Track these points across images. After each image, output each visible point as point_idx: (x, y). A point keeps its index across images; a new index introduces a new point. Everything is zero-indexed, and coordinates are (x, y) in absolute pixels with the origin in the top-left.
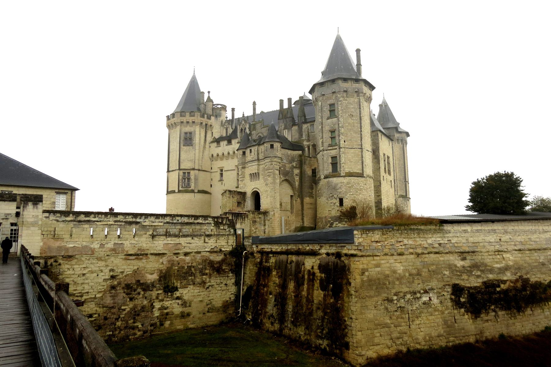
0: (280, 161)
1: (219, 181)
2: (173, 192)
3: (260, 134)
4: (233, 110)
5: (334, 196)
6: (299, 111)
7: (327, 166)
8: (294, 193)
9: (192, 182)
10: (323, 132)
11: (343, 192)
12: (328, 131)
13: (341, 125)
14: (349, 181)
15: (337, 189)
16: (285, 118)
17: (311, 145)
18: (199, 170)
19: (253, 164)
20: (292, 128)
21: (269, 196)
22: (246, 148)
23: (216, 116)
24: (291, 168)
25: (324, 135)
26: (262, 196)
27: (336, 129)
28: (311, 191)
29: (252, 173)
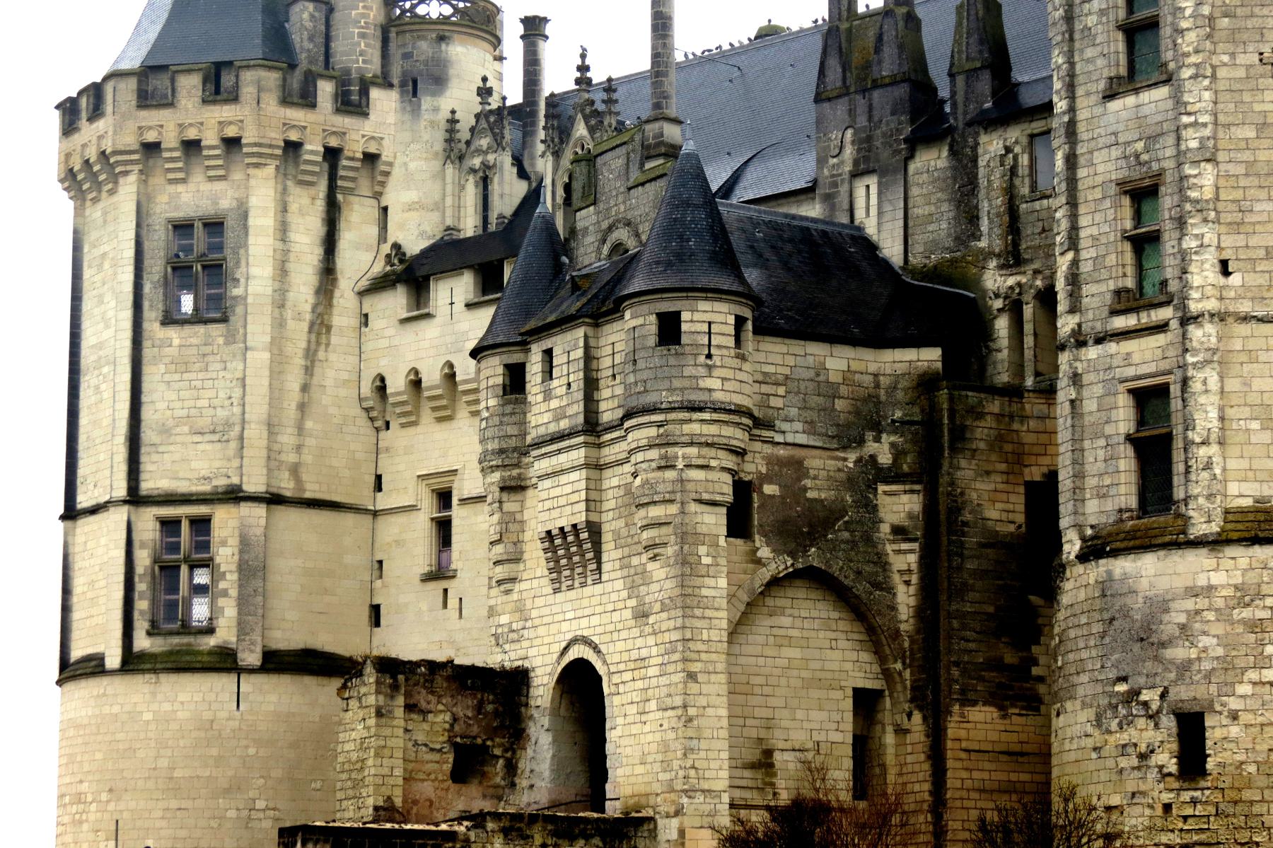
0: (736, 436)
1: (430, 577)
2: (93, 667)
3: (622, 234)
4: (534, 28)
5: (1145, 696)
6: (959, 24)
7: (1101, 466)
8: (887, 674)
10: (1081, 197)
11: (1206, 665)
12: (1113, 189)
13: (1193, 144)
14: (1252, 577)
15: (1163, 645)
16: (864, 91)
17: (1028, 297)
18: (274, 499)
19: (564, 460)
20: (912, 167)
21: (653, 705)
22: (524, 345)
23: (412, 88)
24: (850, 482)
25: (1083, 221)
26: (617, 700)
27: (1160, 174)
28: (1010, 658)
29: (554, 526)
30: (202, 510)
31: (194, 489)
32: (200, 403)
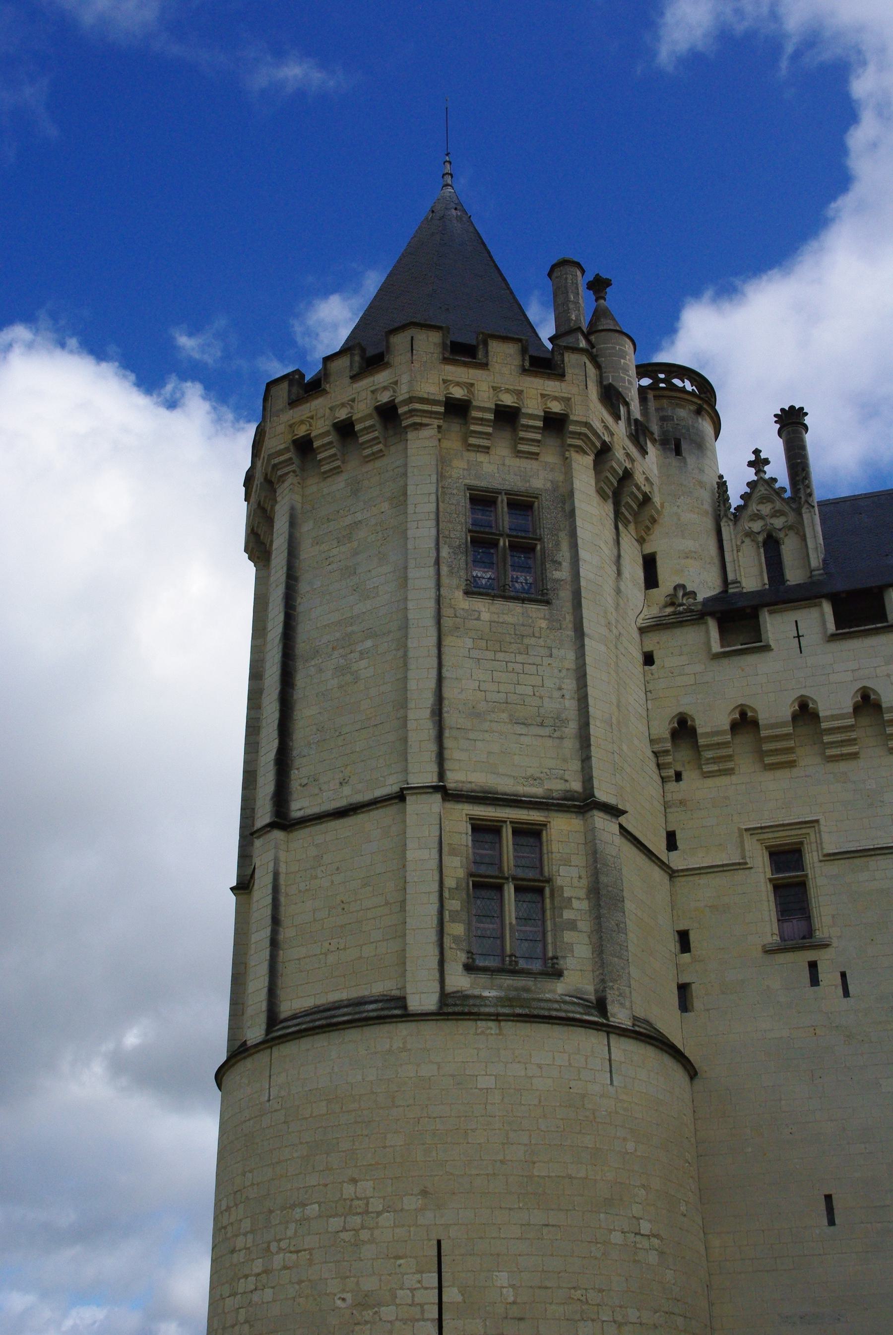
9: (572, 925)
30: (535, 816)
31: (520, 789)
32: (520, 689)
